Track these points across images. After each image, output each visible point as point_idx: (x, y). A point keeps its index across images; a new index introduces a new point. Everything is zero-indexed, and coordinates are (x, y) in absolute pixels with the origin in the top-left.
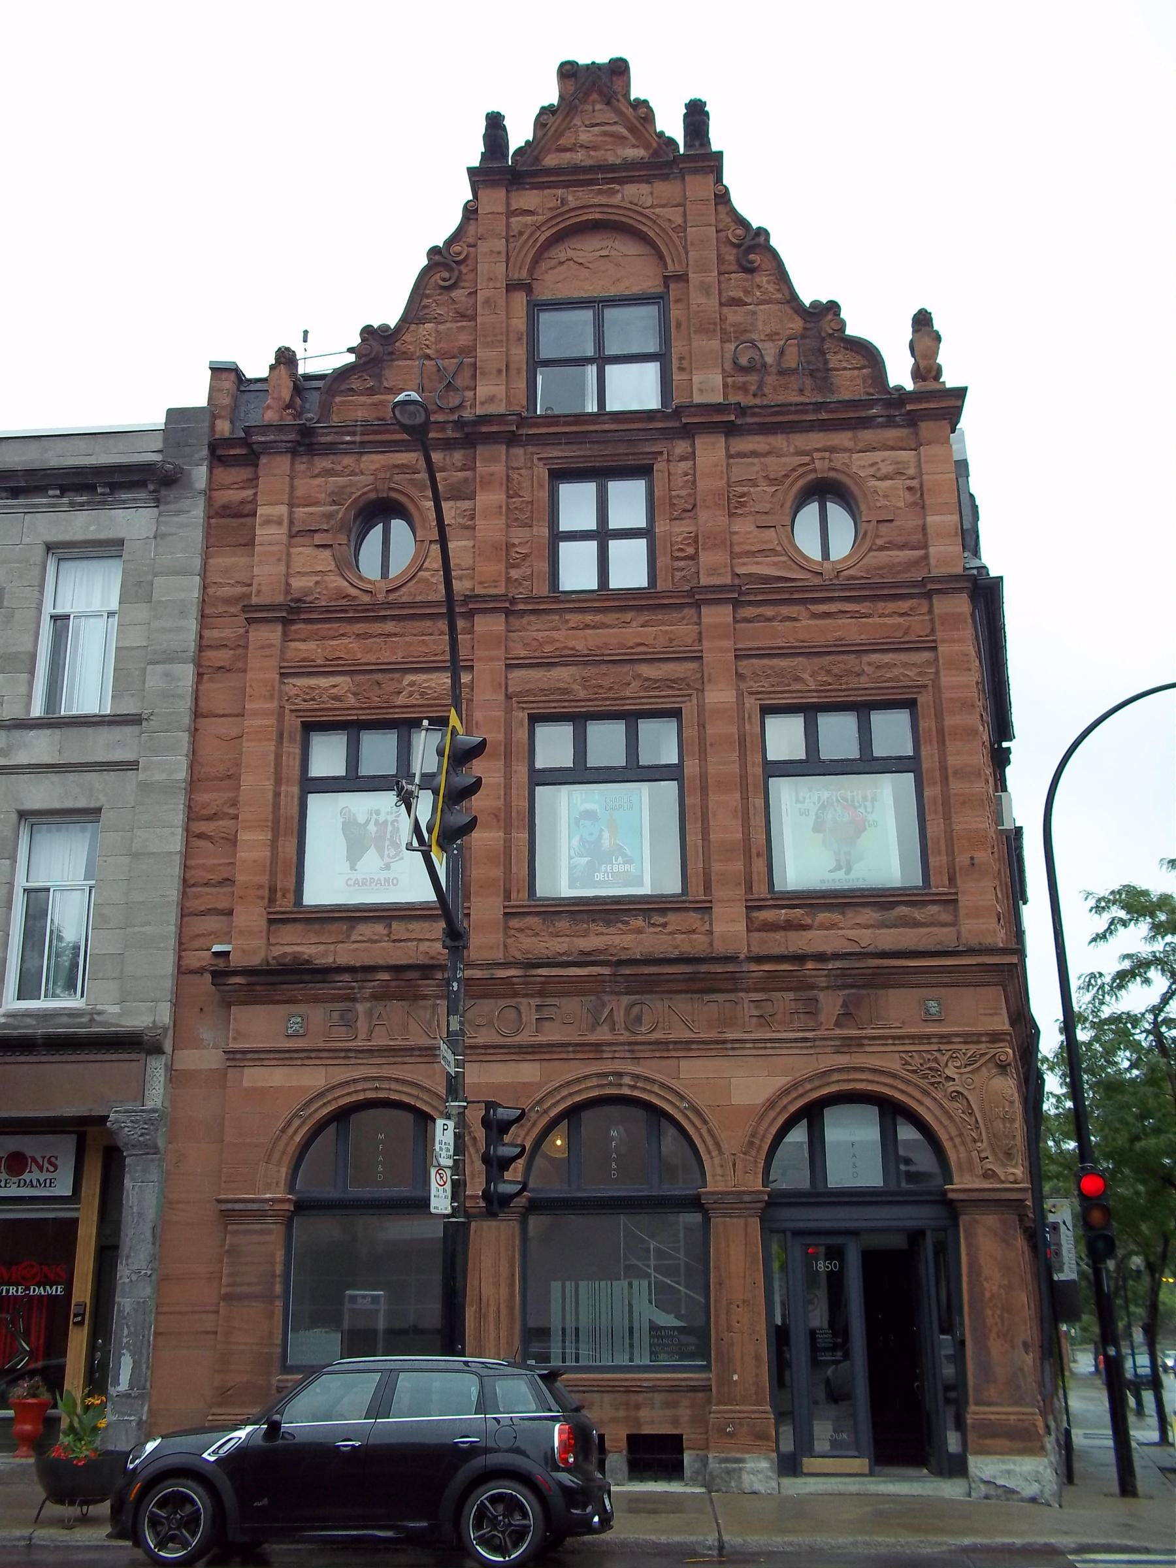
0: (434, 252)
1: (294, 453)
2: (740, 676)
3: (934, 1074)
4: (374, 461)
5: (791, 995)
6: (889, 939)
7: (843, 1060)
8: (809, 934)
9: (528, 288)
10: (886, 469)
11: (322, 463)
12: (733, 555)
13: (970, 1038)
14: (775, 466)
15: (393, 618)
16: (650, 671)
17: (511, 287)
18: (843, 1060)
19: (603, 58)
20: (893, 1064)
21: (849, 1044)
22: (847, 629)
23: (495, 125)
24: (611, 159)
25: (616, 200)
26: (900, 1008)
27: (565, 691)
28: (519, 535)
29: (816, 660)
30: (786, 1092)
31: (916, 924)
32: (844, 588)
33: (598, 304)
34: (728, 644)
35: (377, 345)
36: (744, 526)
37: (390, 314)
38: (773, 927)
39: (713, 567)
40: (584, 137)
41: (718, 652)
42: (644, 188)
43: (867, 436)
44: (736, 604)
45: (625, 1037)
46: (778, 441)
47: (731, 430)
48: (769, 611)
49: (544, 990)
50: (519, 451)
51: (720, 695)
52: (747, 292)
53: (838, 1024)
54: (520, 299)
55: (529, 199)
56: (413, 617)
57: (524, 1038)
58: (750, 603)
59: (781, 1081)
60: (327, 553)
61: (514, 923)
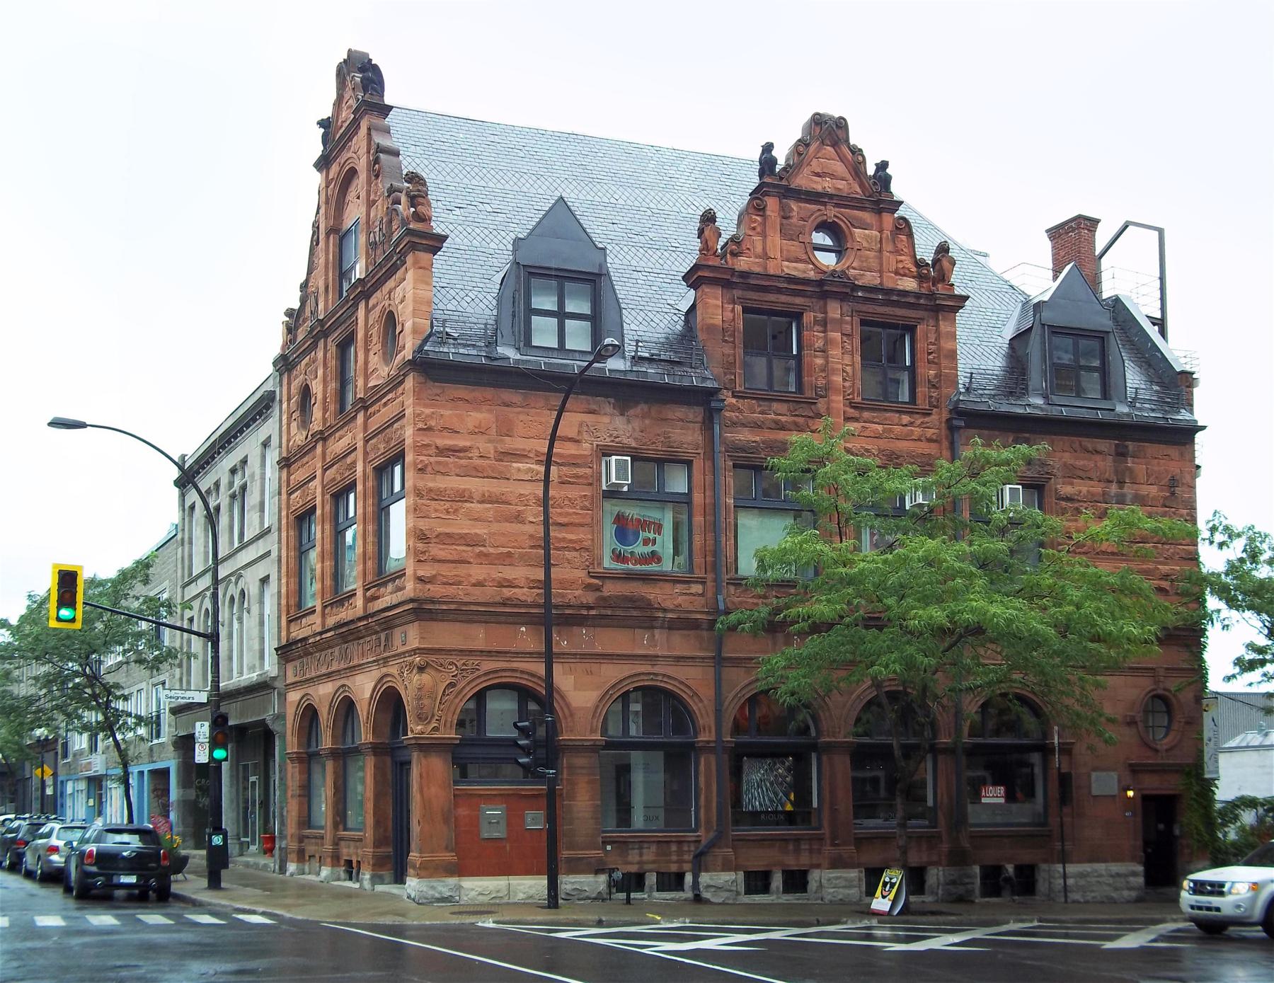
32: (387, 384)
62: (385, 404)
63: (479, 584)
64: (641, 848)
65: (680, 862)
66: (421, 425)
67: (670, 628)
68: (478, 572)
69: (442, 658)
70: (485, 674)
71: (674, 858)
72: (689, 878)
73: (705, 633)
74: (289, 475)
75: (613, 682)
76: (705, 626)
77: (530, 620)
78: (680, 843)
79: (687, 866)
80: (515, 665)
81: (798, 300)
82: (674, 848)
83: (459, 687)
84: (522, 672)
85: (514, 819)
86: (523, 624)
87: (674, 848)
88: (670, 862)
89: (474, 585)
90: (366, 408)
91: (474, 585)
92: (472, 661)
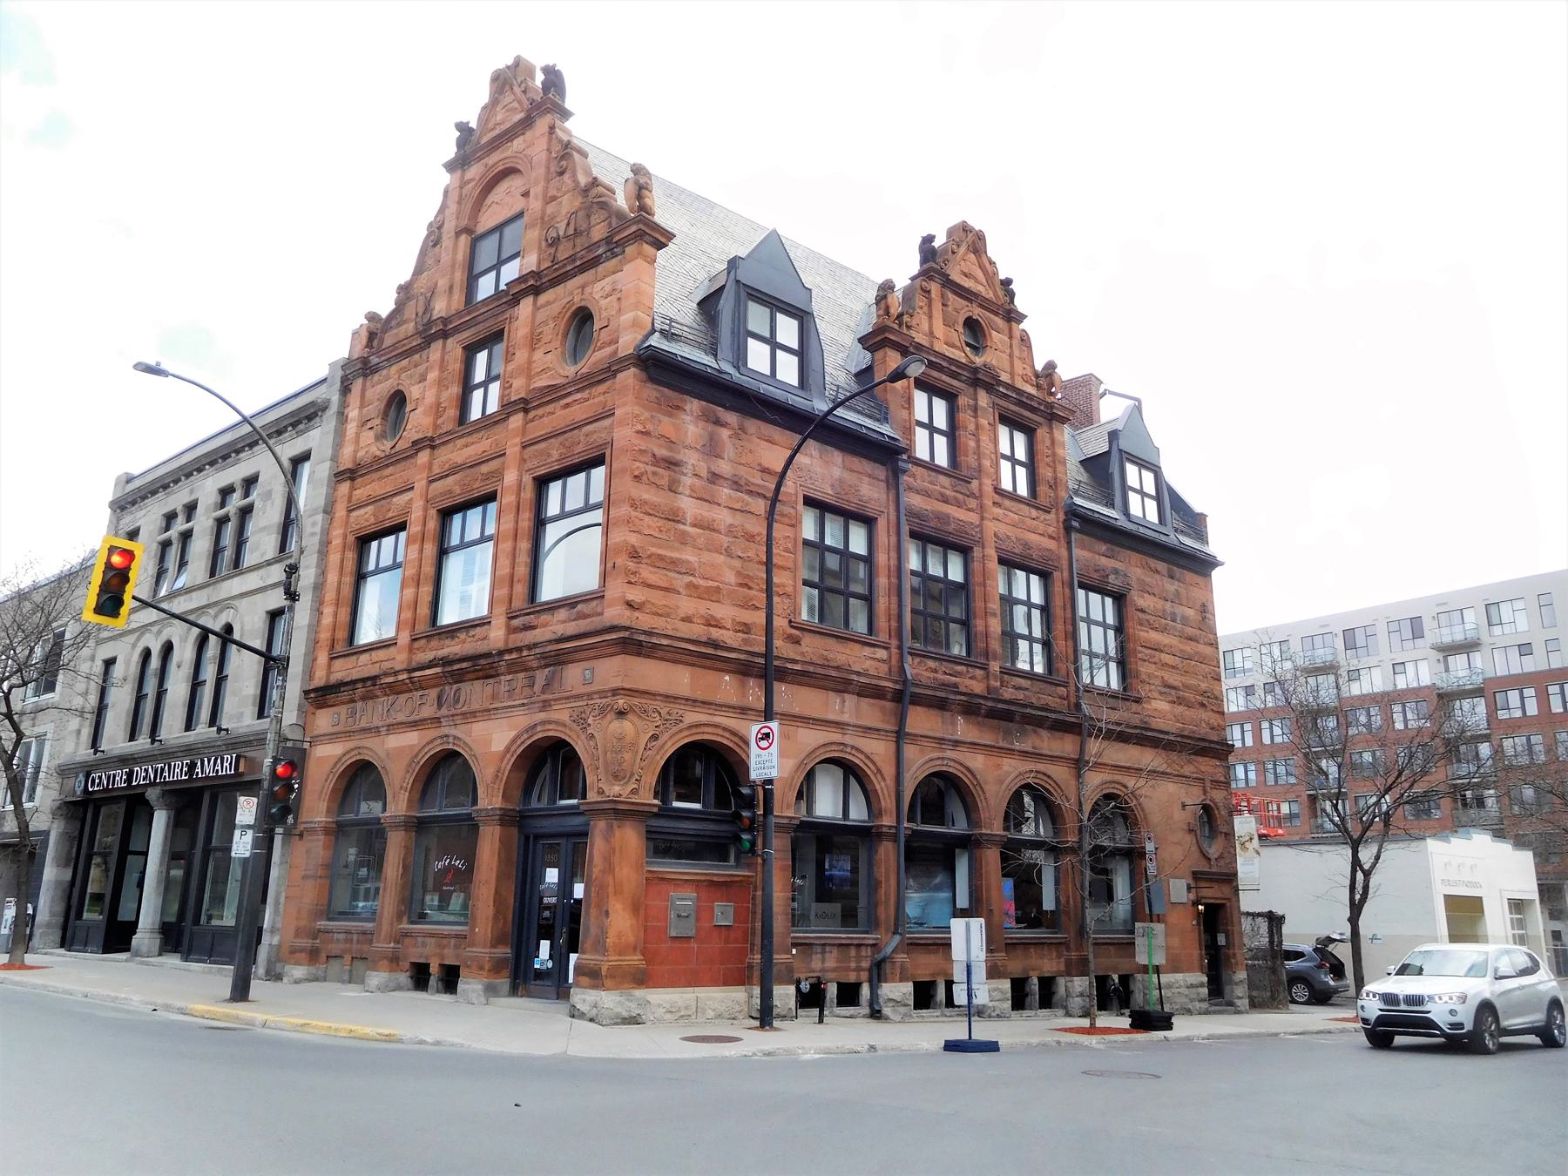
0: (431, 225)
1: (365, 376)
2: (524, 460)
5: (522, 675)
6: (571, 628)
7: (542, 716)
9: (468, 230)
10: (608, 289)
11: (376, 377)
12: (530, 377)
13: (602, 694)
14: (556, 308)
15: (392, 464)
16: (485, 469)
17: (458, 234)
18: (542, 716)
19: (510, 62)
20: (564, 716)
21: (546, 706)
22: (578, 413)
23: (463, 128)
24: (507, 125)
25: (508, 153)
26: (573, 676)
27: (450, 492)
28: (445, 395)
29: (561, 439)
30: (514, 741)
31: (586, 616)
33: (499, 228)
34: (518, 440)
35: (405, 291)
36: (538, 355)
38: (516, 630)
39: (519, 388)
40: (499, 117)
41: (513, 450)
42: (521, 139)
43: (601, 268)
44: (526, 411)
46: (560, 289)
47: (536, 291)
48: (540, 412)
49: (421, 685)
50: (449, 341)
51: (510, 477)
52: (559, 189)
53: (543, 692)
54: (464, 239)
55: (475, 171)
56: (398, 461)
57: (414, 718)
58: (535, 408)
59: (513, 733)
60: (371, 433)
61: (416, 645)
62: (567, 405)
63: (687, 619)
64: (823, 952)
65: (859, 969)
66: (640, 427)
67: (859, 695)
68: (687, 605)
70: (690, 727)
71: (853, 965)
72: (865, 991)
73: (888, 705)
74: (353, 489)
75: (810, 749)
76: (889, 696)
77: (743, 669)
78: (859, 946)
79: (864, 975)
80: (717, 720)
81: (955, 383)
82: (853, 952)
83: (660, 742)
84: (725, 729)
85: (701, 912)
86: (728, 672)
87: (853, 952)
88: (848, 969)
89: (683, 620)
90: (526, 411)
91: (683, 620)
92: (677, 709)
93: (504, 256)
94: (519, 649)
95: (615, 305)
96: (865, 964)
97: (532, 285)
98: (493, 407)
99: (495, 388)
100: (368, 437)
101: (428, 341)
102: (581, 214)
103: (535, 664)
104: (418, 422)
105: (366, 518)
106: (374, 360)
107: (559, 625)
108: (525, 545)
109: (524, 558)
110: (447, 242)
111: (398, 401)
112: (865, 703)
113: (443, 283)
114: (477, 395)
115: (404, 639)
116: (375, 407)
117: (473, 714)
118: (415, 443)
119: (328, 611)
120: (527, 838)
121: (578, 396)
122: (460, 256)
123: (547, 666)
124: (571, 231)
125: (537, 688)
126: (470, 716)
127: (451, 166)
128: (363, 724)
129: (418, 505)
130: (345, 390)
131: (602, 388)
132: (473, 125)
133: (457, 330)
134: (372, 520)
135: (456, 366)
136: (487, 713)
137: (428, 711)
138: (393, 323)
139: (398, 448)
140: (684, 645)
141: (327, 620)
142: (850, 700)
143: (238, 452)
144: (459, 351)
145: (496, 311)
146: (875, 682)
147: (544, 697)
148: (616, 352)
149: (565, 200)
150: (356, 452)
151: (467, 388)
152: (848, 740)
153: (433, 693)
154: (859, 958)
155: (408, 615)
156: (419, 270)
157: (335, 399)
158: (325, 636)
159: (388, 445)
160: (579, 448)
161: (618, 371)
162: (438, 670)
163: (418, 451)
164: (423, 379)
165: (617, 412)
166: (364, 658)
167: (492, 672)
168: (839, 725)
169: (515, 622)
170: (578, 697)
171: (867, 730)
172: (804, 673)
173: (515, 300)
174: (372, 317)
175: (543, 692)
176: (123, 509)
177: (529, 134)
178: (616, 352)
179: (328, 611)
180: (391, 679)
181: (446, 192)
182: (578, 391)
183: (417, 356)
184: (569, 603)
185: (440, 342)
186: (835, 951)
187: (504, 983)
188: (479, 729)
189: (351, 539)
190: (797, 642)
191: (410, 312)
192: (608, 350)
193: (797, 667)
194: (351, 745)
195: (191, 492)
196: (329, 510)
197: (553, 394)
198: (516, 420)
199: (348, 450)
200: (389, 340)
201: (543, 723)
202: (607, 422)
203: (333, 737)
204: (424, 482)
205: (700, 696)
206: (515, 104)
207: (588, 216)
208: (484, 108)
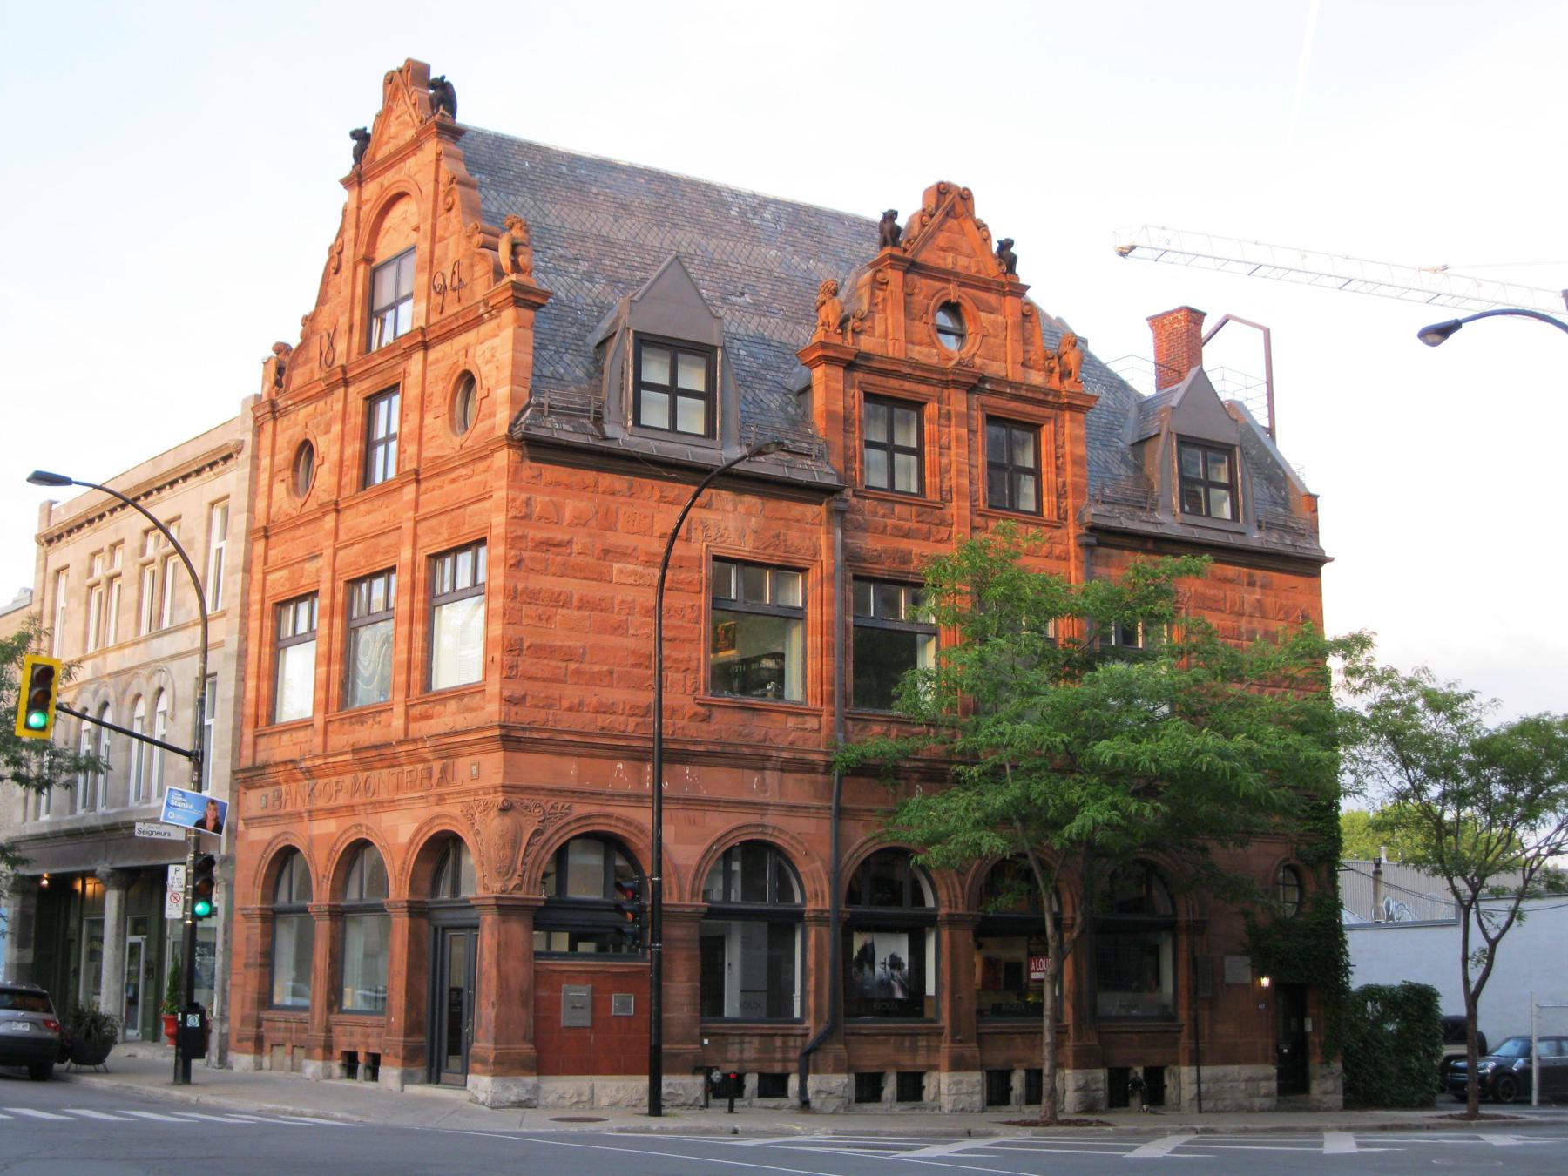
3: (470, 817)
4: (303, 413)
5: (420, 766)
6: (461, 722)
7: (437, 810)
8: (432, 722)
18: (437, 810)
21: (441, 799)
30: (416, 834)
32: (461, 457)
37: (310, 307)
45: (364, 800)
48: (431, 484)
50: (351, 389)
53: (439, 785)
57: (333, 804)
59: (416, 825)
62: (453, 481)
64: (742, 1043)
67: (782, 770)
68: (572, 694)
69: (526, 799)
71: (778, 1055)
72: (794, 1082)
73: (820, 778)
74: (267, 548)
76: (821, 769)
77: (636, 756)
79: (793, 1066)
80: (609, 810)
82: (778, 1042)
84: (618, 819)
87: (778, 1042)
88: (773, 1060)
89: (570, 709)
91: (570, 709)
92: (562, 803)
93: (404, 291)
94: (414, 741)
95: (494, 373)
96: (795, 1055)
97: (423, 341)
98: (392, 474)
99: (394, 445)
100: (280, 490)
101: (331, 388)
102: (465, 262)
103: (429, 756)
104: (324, 478)
105: (280, 584)
106: (281, 403)
107: (447, 719)
108: (419, 628)
109: (418, 643)
110: (346, 271)
111: (306, 449)
112: (791, 779)
113: (343, 322)
114: (381, 450)
115: (319, 722)
116: (285, 454)
117: (381, 804)
118: (321, 506)
119: (251, 684)
120: (436, 929)
121: (463, 471)
122: (359, 291)
123: (441, 758)
124: (456, 283)
125: (434, 781)
126: (379, 806)
127: (347, 183)
128: (289, 809)
129: (326, 575)
130: (258, 430)
131: (482, 465)
132: (369, 131)
133: (357, 378)
134: (288, 586)
135: (356, 420)
136: (391, 804)
137: (342, 799)
138: (300, 361)
139: (306, 509)
140: (567, 737)
141: (251, 695)
142: (771, 777)
143: (159, 489)
144: (360, 402)
145: (393, 362)
146: (798, 755)
147: (440, 790)
148: (492, 429)
149: (452, 241)
150: (269, 506)
151: (369, 444)
152: (767, 820)
153: (347, 779)
154: (785, 1049)
155: (322, 695)
156: (322, 300)
157: (248, 438)
158: (250, 710)
159: (299, 502)
160: (466, 529)
161: (493, 451)
162: (349, 757)
163: (325, 514)
164: (327, 431)
165: (496, 495)
166: (285, 737)
167: (395, 762)
168: (761, 807)
169: (413, 711)
170: (467, 792)
171: (793, 809)
172: (710, 754)
173: (407, 354)
174: (281, 349)
175: (439, 785)
176: (50, 542)
177: (420, 155)
178: (492, 429)
179: (251, 684)
180: (308, 764)
181: (345, 211)
182: (463, 465)
183: (321, 404)
184: (459, 694)
185: (342, 390)
186: (756, 1041)
187: (421, 1072)
188: (388, 819)
189: (269, 604)
190: (706, 719)
191: (314, 351)
192: (488, 423)
193: (701, 748)
194: (278, 829)
195: (117, 531)
196: (247, 570)
197: (441, 468)
198: (409, 491)
199: (261, 505)
200: (298, 378)
201: (439, 817)
202: (487, 504)
203: (262, 820)
204: (330, 551)
205: (588, 786)
206: (407, 117)
207: (472, 266)
208: (378, 116)
